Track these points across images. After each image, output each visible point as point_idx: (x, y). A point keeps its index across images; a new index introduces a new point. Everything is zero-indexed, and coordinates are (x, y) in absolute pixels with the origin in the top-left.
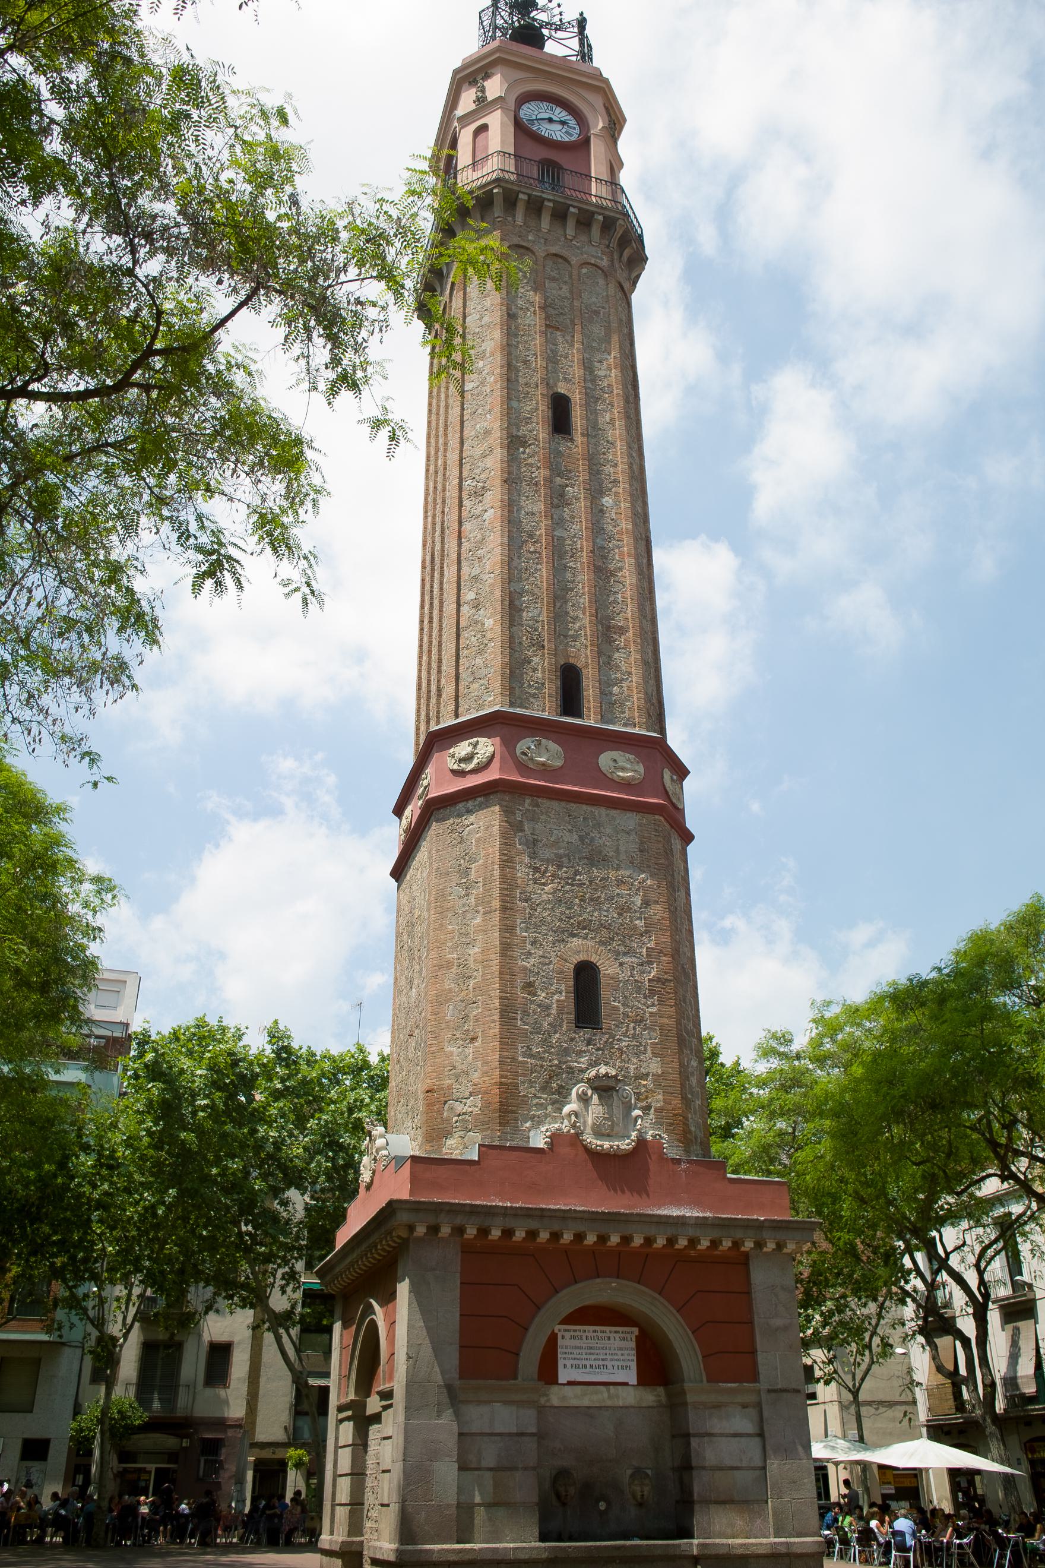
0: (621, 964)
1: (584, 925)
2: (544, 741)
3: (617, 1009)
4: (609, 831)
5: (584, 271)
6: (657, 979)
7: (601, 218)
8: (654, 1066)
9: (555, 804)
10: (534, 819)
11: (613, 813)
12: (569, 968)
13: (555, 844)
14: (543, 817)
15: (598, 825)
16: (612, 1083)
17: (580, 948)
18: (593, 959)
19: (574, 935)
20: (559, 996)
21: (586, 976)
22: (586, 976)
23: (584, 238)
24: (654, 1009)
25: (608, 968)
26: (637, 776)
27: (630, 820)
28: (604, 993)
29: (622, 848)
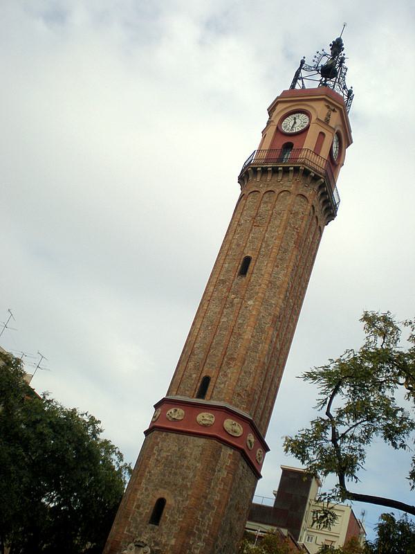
0: (175, 501)
1: (168, 483)
2: (178, 409)
3: (167, 517)
4: (191, 446)
5: (282, 194)
6: (187, 507)
7: (292, 168)
8: (173, 542)
9: (174, 435)
10: (164, 441)
11: (196, 438)
12: (155, 501)
13: (168, 451)
14: (168, 440)
15: (187, 444)
16: (141, 545)
17: (162, 493)
18: (166, 497)
19: (161, 487)
20: (148, 510)
21: (161, 503)
22: (161, 503)
23: (286, 179)
24: (181, 519)
25: (170, 501)
26: (210, 423)
27: (201, 441)
28: (165, 510)
29: (194, 453)
